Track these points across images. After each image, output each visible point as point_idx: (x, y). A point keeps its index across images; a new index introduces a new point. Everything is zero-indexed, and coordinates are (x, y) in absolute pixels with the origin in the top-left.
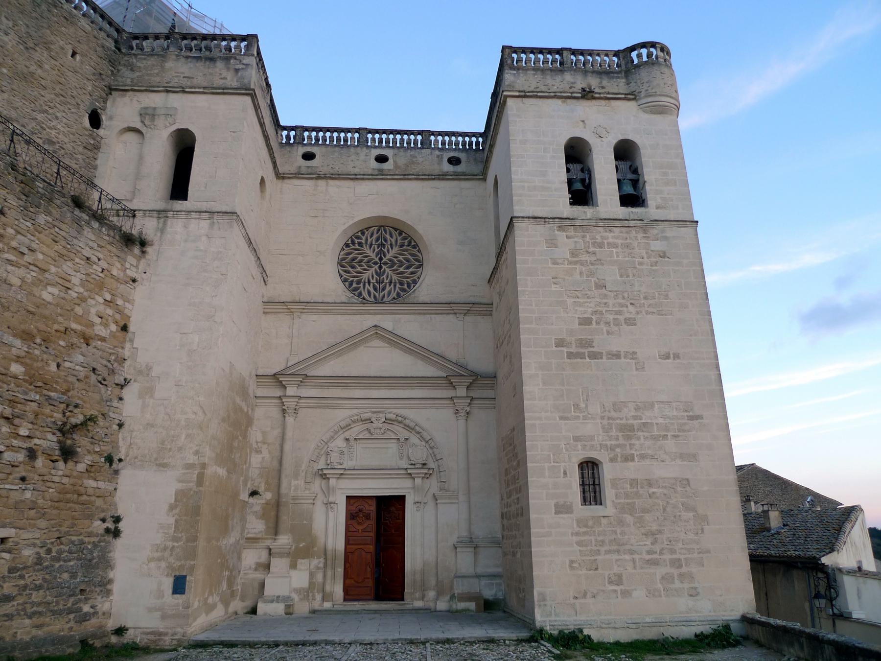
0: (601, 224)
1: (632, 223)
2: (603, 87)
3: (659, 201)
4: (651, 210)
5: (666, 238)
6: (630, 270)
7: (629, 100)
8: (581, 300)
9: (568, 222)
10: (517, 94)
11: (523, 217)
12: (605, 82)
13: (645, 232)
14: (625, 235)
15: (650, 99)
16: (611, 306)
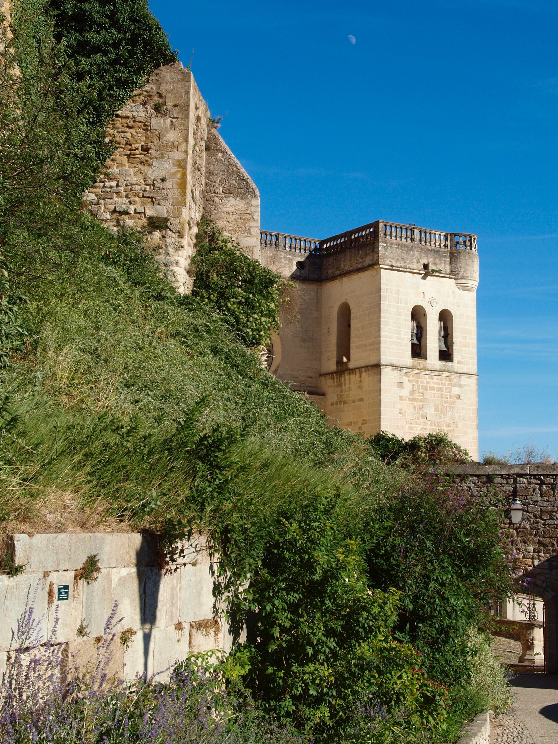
0: (428, 373)
2: (436, 264)
3: (460, 359)
5: (460, 386)
7: (451, 278)
9: (410, 371)
10: (387, 267)
12: (437, 261)
15: (464, 281)
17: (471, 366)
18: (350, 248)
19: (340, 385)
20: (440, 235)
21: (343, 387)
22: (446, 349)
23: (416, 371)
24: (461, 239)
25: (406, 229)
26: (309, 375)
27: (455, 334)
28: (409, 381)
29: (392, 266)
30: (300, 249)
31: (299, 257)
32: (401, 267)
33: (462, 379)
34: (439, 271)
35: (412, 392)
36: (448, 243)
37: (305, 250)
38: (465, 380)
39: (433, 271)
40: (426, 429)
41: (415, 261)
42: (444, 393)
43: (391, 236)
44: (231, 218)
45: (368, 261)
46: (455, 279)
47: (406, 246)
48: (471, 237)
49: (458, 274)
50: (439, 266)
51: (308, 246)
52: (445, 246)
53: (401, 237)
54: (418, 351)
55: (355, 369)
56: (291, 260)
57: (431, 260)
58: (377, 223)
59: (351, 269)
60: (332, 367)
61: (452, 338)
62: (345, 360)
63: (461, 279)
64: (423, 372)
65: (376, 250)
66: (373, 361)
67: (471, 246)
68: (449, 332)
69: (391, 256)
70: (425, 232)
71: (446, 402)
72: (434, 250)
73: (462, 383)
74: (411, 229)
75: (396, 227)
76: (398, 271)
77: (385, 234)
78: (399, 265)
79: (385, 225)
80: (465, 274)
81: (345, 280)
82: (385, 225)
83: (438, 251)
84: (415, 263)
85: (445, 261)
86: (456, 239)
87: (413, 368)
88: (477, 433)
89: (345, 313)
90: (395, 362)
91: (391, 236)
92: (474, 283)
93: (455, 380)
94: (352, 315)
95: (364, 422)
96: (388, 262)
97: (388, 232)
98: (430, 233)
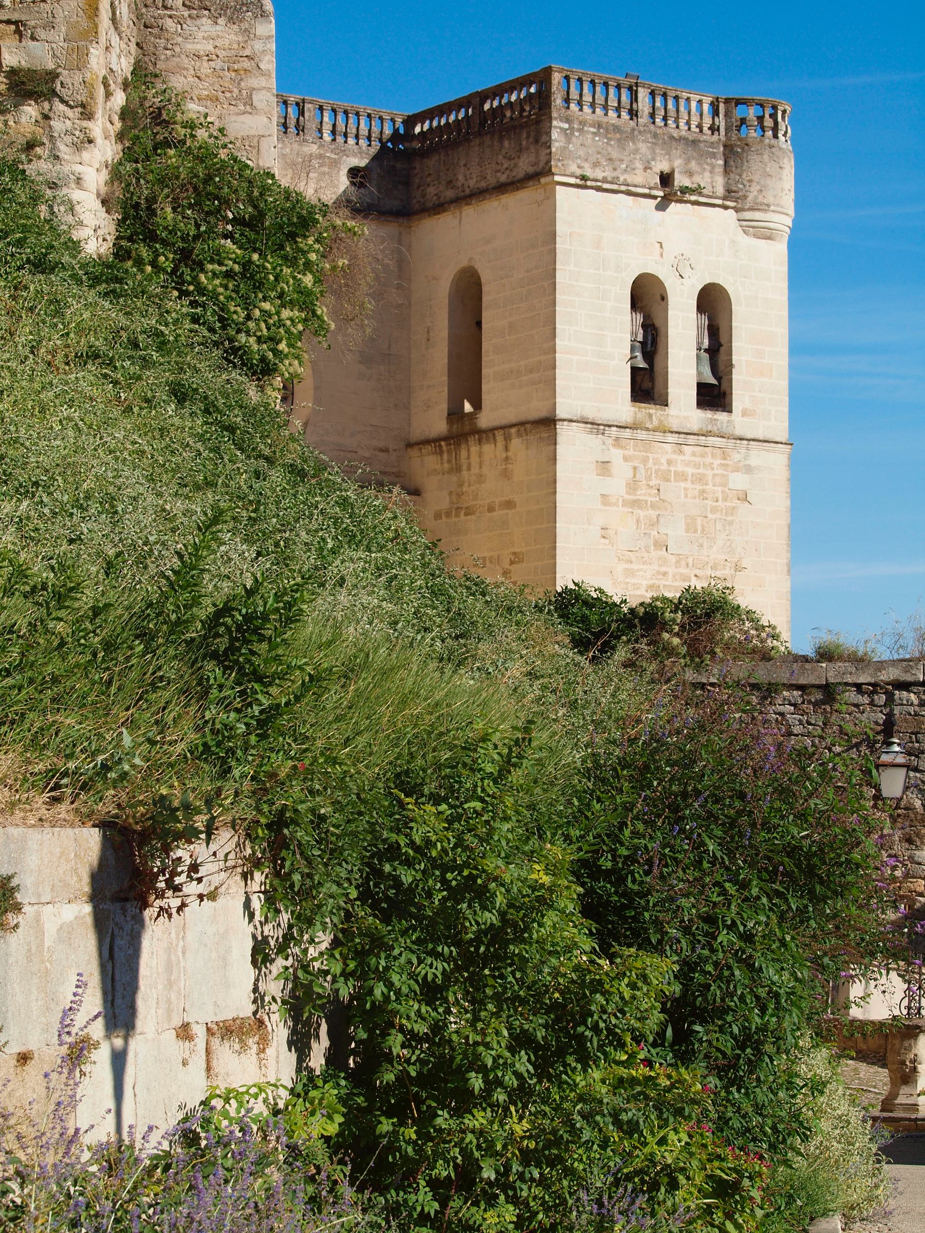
0: (671, 438)
1: (711, 440)
2: (690, 174)
4: (737, 419)
5: (749, 469)
6: (699, 521)
7: (726, 208)
8: (635, 566)
9: (627, 433)
10: (572, 181)
11: (571, 421)
12: (693, 165)
13: (725, 456)
14: (697, 459)
15: (757, 215)
16: (670, 577)
17: (776, 423)
18: (480, 134)
19: (458, 469)
20: (700, 102)
21: (464, 473)
22: (713, 381)
23: (641, 435)
24: (752, 113)
25: (618, 87)
26: (381, 444)
27: (735, 344)
28: (626, 459)
29: (584, 178)
30: (357, 137)
31: (355, 155)
32: (605, 180)
33: (753, 453)
34: (698, 191)
35: (632, 486)
36: (721, 121)
37: (369, 138)
38: (759, 456)
39: (685, 190)
40: (665, 574)
41: (639, 165)
42: (710, 487)
43: (580, 103)
44: (205, 68)
45: (524, 165)
46: (737, 210)
47: (616, 129)
48: (775, 108)
49: (745, 197)
50: (697, 179)
51: (376, 130)
52: (714, 129)
53: (605, 107)
54: (647, 386)
55: (493, 430)
56: (335, 164)
57: (678, 163)
58: (547, 73)
59: (483, 184)
60: (436, 423)
61: (730, 353)
62: (468, 407)
63: (751, 209)
64: (659, 436)
65: (544, 138)
66: (536, 410)
67: (775, 129)
68: (723, 340)
69: (581, 152)
70: (665, 95)
71: (714, 510)
72: (685, 139)
73: (754, 461)
74: (630, 88)
75: (593, 82)
76: (599, 189)
77: (567, 100)
78: (600, 175)
79: (567, 78)
80: (760, 199)
81: (469, 212)
82: (567, 78)
83: (695, 142)
84: (639, 172)
85: (713, 166)
86: (739, 112)
87: (634, 427)
88: (788, 584)
89: (469, 293)
90: (591, 415)
91: (580, 103)
92: (782, 219)
93: (736, 457)
94: (486, 299)
95: (517, 558)
96: (573, 168)
97: (574, 94)
98: (676, 98)
